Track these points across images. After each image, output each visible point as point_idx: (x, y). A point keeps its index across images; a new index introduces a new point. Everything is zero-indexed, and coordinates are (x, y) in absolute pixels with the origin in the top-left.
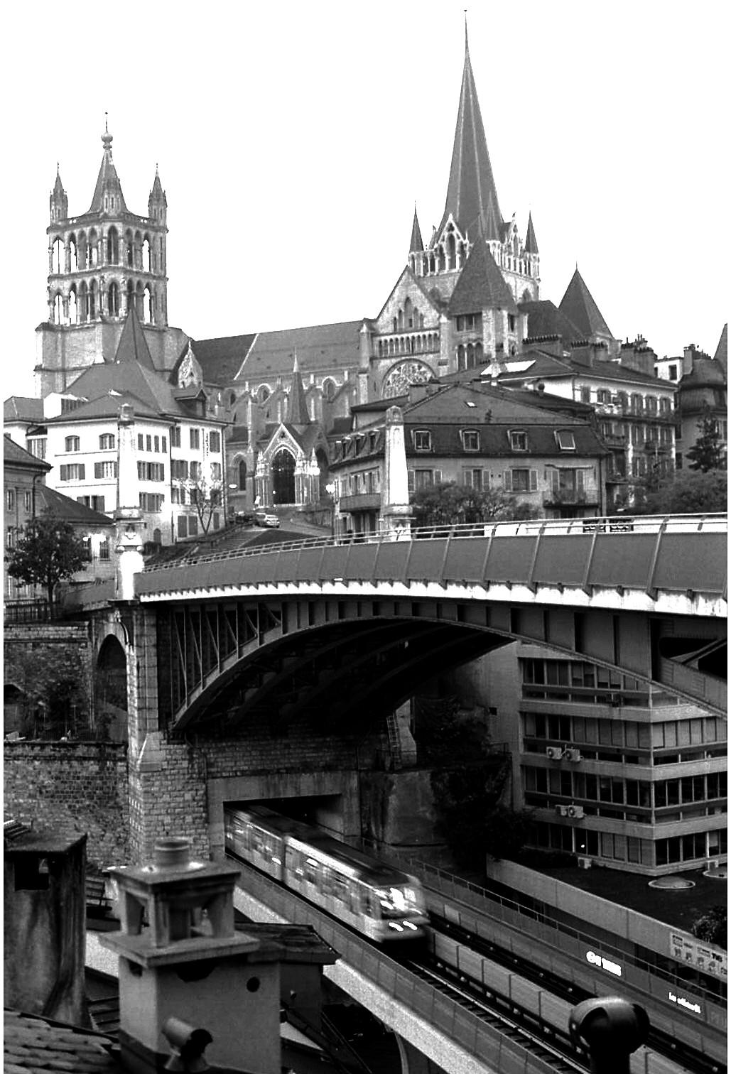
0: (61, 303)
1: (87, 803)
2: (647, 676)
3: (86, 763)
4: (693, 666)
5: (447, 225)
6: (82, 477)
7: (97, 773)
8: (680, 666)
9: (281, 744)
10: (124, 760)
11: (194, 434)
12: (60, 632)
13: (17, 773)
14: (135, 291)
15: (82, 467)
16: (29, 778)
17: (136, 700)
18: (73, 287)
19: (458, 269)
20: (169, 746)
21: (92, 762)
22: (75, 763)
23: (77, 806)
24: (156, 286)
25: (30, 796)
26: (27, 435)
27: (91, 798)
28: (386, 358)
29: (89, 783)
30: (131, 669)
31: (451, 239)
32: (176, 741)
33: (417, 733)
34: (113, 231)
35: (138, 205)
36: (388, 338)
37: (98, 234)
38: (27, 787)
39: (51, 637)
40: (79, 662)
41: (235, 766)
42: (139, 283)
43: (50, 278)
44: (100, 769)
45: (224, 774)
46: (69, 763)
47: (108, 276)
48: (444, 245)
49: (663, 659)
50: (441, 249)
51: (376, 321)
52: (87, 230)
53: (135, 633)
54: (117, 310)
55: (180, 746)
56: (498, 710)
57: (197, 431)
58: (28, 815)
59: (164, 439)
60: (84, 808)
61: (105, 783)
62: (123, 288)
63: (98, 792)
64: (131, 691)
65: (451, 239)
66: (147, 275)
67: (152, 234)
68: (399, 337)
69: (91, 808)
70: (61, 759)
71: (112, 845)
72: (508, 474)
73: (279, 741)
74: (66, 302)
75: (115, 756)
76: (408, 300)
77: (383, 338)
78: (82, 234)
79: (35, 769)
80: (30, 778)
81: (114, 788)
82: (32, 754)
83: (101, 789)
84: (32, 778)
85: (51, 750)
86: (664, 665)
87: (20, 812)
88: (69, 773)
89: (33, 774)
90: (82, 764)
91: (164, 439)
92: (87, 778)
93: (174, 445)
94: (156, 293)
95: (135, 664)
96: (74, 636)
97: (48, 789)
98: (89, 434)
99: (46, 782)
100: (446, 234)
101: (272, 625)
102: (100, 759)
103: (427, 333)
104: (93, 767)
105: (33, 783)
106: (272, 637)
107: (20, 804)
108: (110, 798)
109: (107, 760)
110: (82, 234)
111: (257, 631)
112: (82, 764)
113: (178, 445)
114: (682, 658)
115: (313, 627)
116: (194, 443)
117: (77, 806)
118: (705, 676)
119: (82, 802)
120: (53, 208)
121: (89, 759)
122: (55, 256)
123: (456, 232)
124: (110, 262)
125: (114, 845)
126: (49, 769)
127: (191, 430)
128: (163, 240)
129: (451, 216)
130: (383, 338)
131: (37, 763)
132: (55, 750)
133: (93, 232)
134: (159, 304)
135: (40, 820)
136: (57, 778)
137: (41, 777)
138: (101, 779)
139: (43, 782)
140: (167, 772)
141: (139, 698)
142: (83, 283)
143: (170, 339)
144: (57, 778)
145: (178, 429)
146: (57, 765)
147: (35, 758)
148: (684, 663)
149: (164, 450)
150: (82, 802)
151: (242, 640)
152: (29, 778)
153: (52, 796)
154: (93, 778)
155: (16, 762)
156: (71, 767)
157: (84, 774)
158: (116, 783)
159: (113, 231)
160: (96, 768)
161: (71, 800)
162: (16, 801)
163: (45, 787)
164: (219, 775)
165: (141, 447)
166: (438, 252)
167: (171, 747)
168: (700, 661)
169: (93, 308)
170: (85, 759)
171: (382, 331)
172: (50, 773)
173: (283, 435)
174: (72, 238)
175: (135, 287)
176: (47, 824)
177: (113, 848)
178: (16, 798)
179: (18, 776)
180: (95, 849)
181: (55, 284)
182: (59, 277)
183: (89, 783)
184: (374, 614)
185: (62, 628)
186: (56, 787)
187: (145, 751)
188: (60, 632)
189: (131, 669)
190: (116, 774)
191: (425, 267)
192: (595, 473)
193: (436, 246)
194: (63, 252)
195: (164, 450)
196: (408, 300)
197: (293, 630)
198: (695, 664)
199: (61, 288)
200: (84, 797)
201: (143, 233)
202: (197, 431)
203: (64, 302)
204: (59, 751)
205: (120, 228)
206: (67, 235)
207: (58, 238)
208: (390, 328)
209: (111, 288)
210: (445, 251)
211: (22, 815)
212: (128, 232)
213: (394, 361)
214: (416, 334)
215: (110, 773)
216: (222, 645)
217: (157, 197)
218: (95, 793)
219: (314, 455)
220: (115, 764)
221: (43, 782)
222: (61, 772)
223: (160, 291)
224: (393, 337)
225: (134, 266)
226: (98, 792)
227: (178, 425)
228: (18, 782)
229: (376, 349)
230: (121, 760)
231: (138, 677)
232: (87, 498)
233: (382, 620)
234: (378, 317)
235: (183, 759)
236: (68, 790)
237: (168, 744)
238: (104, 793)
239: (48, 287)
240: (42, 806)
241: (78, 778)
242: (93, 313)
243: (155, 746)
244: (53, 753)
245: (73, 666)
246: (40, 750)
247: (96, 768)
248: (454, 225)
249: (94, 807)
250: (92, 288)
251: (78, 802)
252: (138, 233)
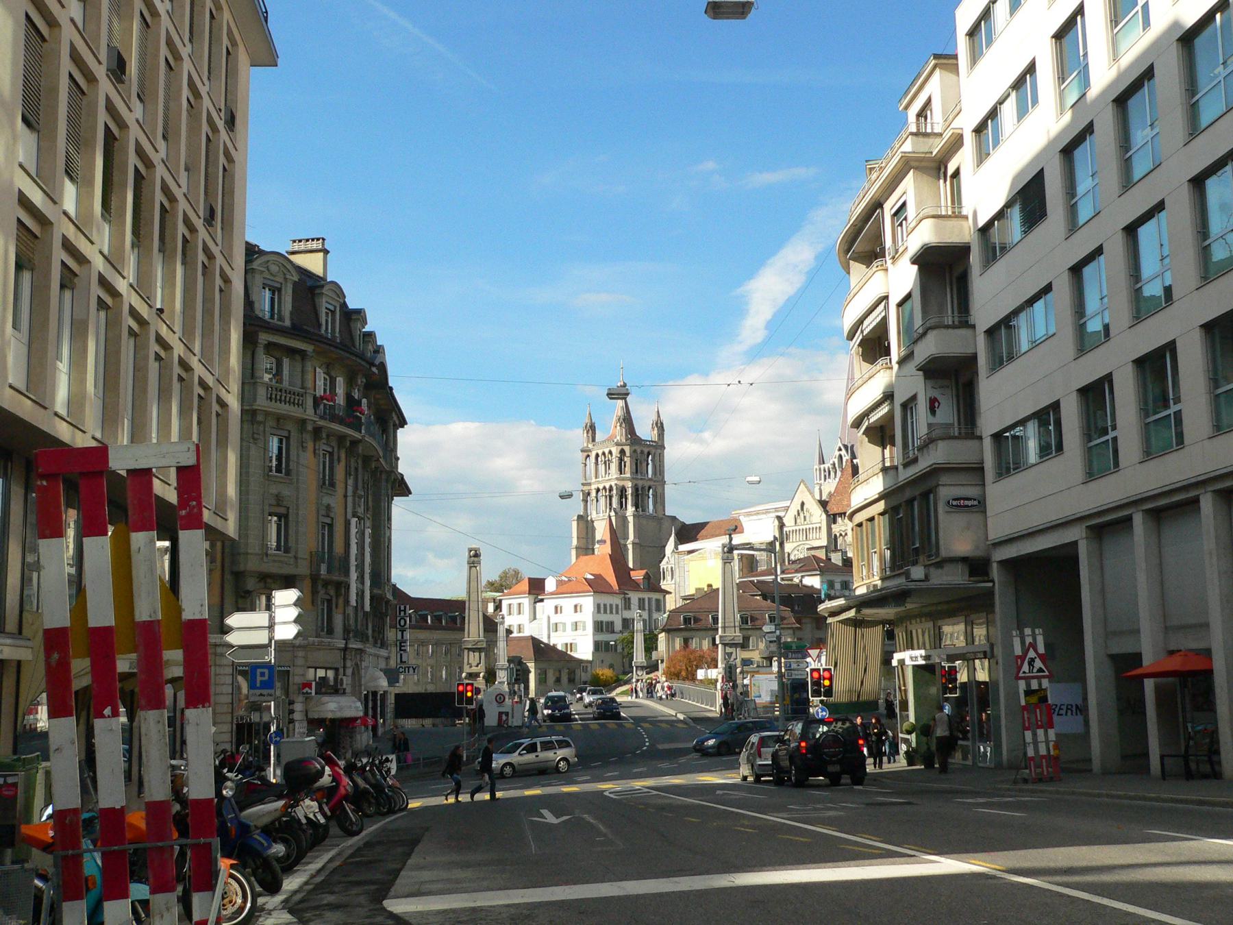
11: (641, 601)
14: (640, 492)
19: (837, 479)
31: (841, 457)
34: (622, 452)
35: (645, 431)
36: (791, 529)
42: (643, 488)
47: (621, 483)
48: (836, 461)
50: (834, 464)
52: (607, 451)
57: (644, 599)
59: (617, 606)
62: (629, 491)
65: (841, 457)
66: (650, 480)
67: (653, 451)
68: (797, 528)
76: (803, 504)
78: (604, 454)
91: (617, 606)
93: (625, 609)
98: (567, 603)
100: (837, 453)
103: (814, 526)
110: (604, 454)
113: (630, 609)
120: (585, 435)
122: (588, 467)
123: (843, 452)
124: (621, 473)
127: (639, 599)
128: (661, 456)
133: (610, 452)
134: (660, 500)
143: (666, 524)
145: (629, 599)
149: (617, 613)
165: (599, 611)
169: (611, 504)
171: (787, 524)
174: (597, 455)
175: (640, 489)
191: (825, 476)
193: (831, 462)
195: (617, 613)
196: (803, 504)
201: (646, 451)
202: (644, 599)
206: (593, 455)
208: (793, 524)
209: (622, 491)
210: (837, 465)
212: (635, 451)
213: (795, 544)
214: (808, 527)
217: (660, 426)
223: (659, 491)
224: (794, 528)
225: (639, 474)
227: (627, 596)
232: (567, 644)
242: (610, 509)
248: (842, 448)
252: (642, 452)
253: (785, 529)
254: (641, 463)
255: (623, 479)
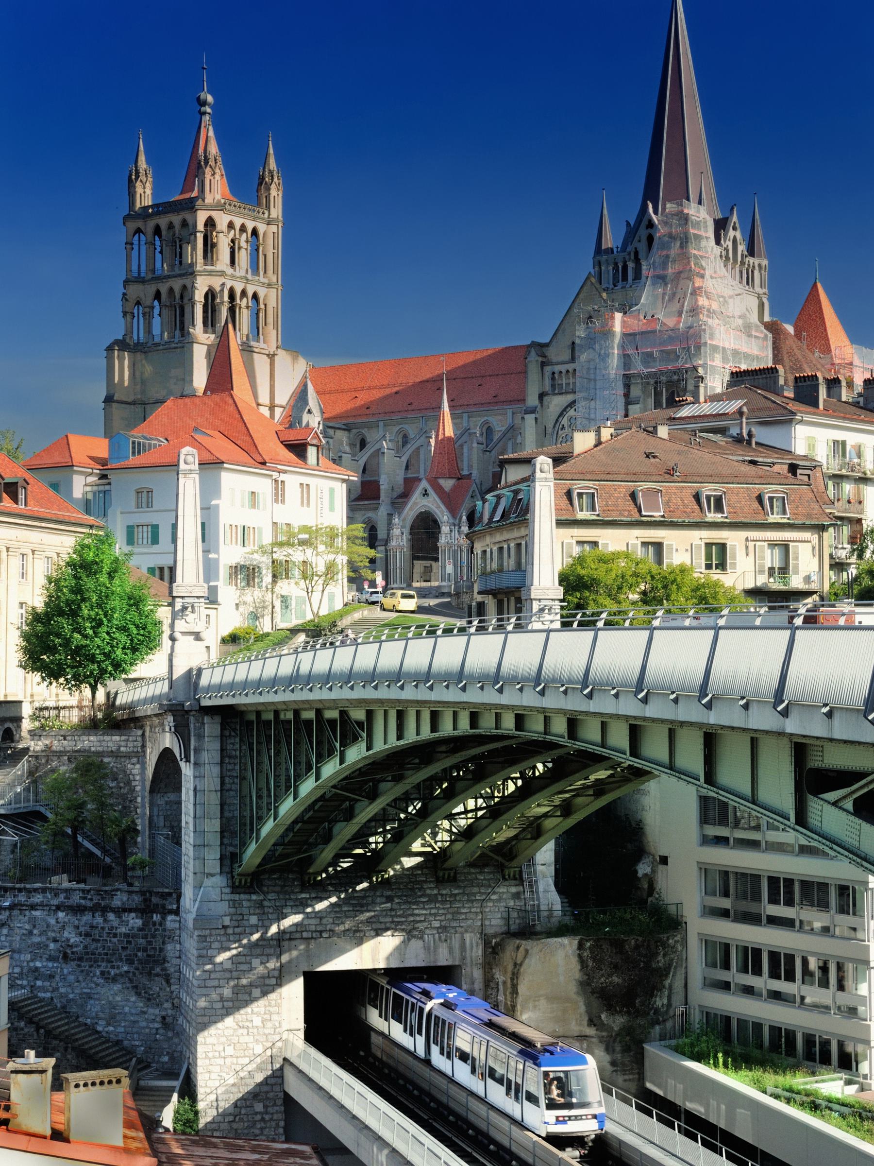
0: (141, 315)
1: (126, 968)
2: (789, 820)
3: (125, 916)
4: (845, 807)
5: (645, 223)
6: (155, 540)
7: (140, 929)
8: (830, 806)
9: (382, 896)
10: (177, 912)
12: (104, 744)
13: (34, 926)
15: (155, 528)
16: (49, 934)
17: (192, 834)
18: (158, 296)
20: (233, 897)
21: (133, 915)
22: (111, 916)
23: (112, 973)
24: (266, 296)
25: (51, 959)
26: (86, 485)
27: (130, 962)
28: (561, 394)
29: (129, 942)
30: (187, 793)
32: (243, 890)
33: (562, 884)
36: (563, 368)
37: (191, 227)
38: (47, 946)
39: (93, 749)
40: (128, 783)
41: (321, 924)
43: (126, 282)
44: (143, 924)
45: (305, 935)
46: (103, 915)
49: (810, 797)
51: (547, 345)
53: (192, 747)
54: (213, 325)
55: (247, 896)
56: (669, 860)
58: (47, 984)
60: (121, 975)
61: (150, 943)
63: (139, 954)
64: (187, 823)
69: (131, 974)
70: (93, 909)
71: (157, 1025)
72: (699, 547)
73: (378, 893)
74: (148, 316)
75: (163, 906)
77: (557, 368)
78: (171, 226)
79: (58, 922)
80: (51, 934)
81: (161, 950)
82: (55, 902)
83: (145, 950)
84: (53, 935)
85: (81, 898)
86: (810, 803)
87: (36, 979)
88: (103, 928)
89: (55, 928)
90: (120, 917)
92: (126, 935)
93: (276, 501)
94: (265, 305)
95: (192, 788)
96: (122, 749)
97: (75, 950)
99: (72, 940)
101: (355, 739)
102: (145, 910)
104: (134, 921)
105: (55, 941)
106: (356, 754)
107: (37, 969)
108: (156, 962)
109: (153, 912)
110: (171, 226)
111: (338, 745)
112: (120, 917)
113: (283, 502)
114: (832, 796)
115: (402, 742)
116: (305, 500)
117: (112, 973)
118: (861, 821)
119: (118, 967)
121: (130, 910)
122: (135, 253)
125: (159, 1026)
126: (77, 922)
127: (301, 484)
129: (651, 210)
130: (557, 368)
131: (61, 915)
132: (85, 898)
133: (184, 224)
135: (62, 990)
136: (87, 935)
137: (66, 934)
138: (145, 937)
139: (68, 940)
140: (230, 931)
141: (195, 832)
142: (171, 290)
144: (87, 935)
146: (87, 918)
147: (58, 908)
148: (835, 804)
150: (118, 967)
151: (320, 758)
152: (49, 934)
153: (80, 959)
154: (134, 936)
155: (33, 912)
156: (105, 920)
157: (123, 930)
158: (164, 943)
159: (210, 223)
160: (139, 922)
161: (104, 964)
162: (32, 964)
163: (71, 946)
164: (298, 935)
166: (632, 257)
167: (236, 897)
168: (855, 801)
170: (125, 910)
172: (77, 927)
173: (425, 494)
174: (157, 231)
176: (71, 996)
177: (157, 1029)
178: (32, 960)
179: (35, 932)
180: (135, 1030)
181: (135, 291)
182: (140, 280)
183: (129, 942)
184: (471, 728)
185: (107, 738)
186: (86, 947)
187: (200, 902)
188: (104, 744)
189: (187, 793)
190: (164, 930)
192: (814, 548)
194: (143, 248)
197: (379, 746)
198: (849, 805)
199: (142, 296)
200: (121, 960)
201: (250, 225)
203: (144, 314)
204: (91, 900)
205: (222, 220)
207: (138, 231)
208: (567, 356)
210: (640, 257)
211: (39, 983)
212: (231, 225)
215: (156, 930)
216: (297, 763)
218: (136, 956)
219: (464, 518)
220: (164, 918)
221: (68, 940)
222: (92, 927)
226: (139, 954)
228: (36, 939)
229: (547, 382)
230: (171, 912)
231: (195, 804)
233: (480, 736)
234: (551, 341)
235: (250, 914)
236: (100, 950)
237: (232, 893)
238: (148, 956)
239: (124, 294)
240: (65, 971)
241: (115, 935)
243: (215, 894)
244: (83, 902)
245: (121, 788)
246: (66, 898)
247: (139, 922)
249: (134, 974)
250: (182, 297)
251: (113, 967)
252: (243, 229)
253: (548, 369)
254: (240, 248)
255: (211, 274)
